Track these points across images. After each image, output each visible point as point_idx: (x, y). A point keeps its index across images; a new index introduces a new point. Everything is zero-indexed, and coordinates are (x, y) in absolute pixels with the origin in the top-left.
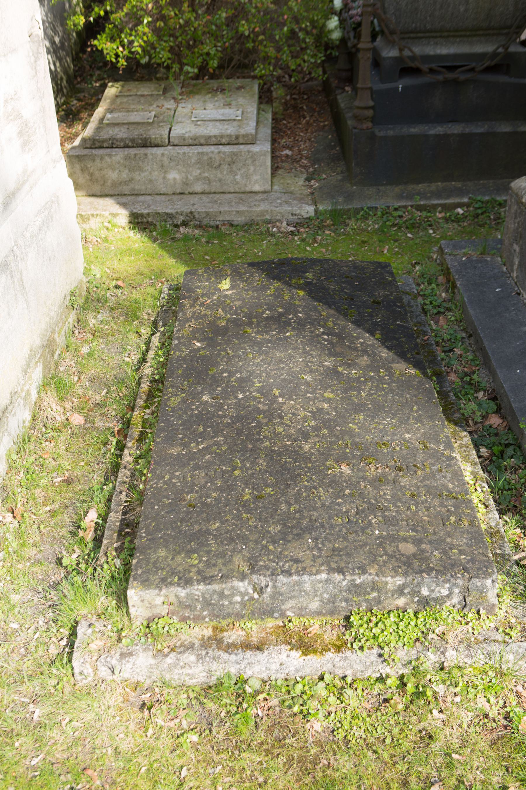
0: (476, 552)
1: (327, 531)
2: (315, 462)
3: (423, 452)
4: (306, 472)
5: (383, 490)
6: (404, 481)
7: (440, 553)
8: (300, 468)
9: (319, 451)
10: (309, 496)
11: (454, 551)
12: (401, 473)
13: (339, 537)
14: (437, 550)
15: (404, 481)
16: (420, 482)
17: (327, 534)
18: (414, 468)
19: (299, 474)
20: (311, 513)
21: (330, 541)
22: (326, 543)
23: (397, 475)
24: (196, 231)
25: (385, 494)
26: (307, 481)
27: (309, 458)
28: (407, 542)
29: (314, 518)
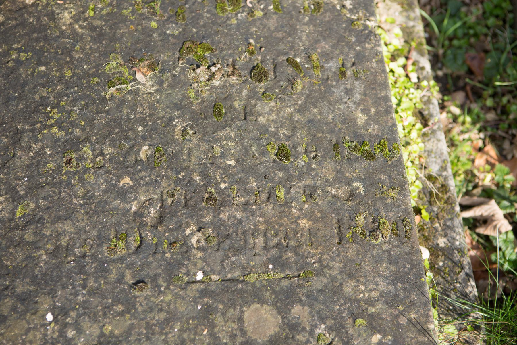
0: (403, 321)
1: (92, 283)
2: (80, 61)
3: (312, 20)
4: (59, 96)
5: (219, 140)
6: (267, 112)
7: (330, 330)
8: (48, 83)
9: (92, 28)
10: (59, 169)
11: (360, 321)
12: (261, 87)
13: (117, 301)
14: (323, 320)
15: (267, 112)
16: (301, 110)
17: (92, 293)
18: (290, 70)
19: (44, 102)
20: (59, 226)
21: (94, 318)
22: (86, 323)
23: (253, 94)
24: (108, 9)
25: (223, 155)
26: (59, 125)
27: (68, 51)
28: (262, 301)
29: (64, 241)
